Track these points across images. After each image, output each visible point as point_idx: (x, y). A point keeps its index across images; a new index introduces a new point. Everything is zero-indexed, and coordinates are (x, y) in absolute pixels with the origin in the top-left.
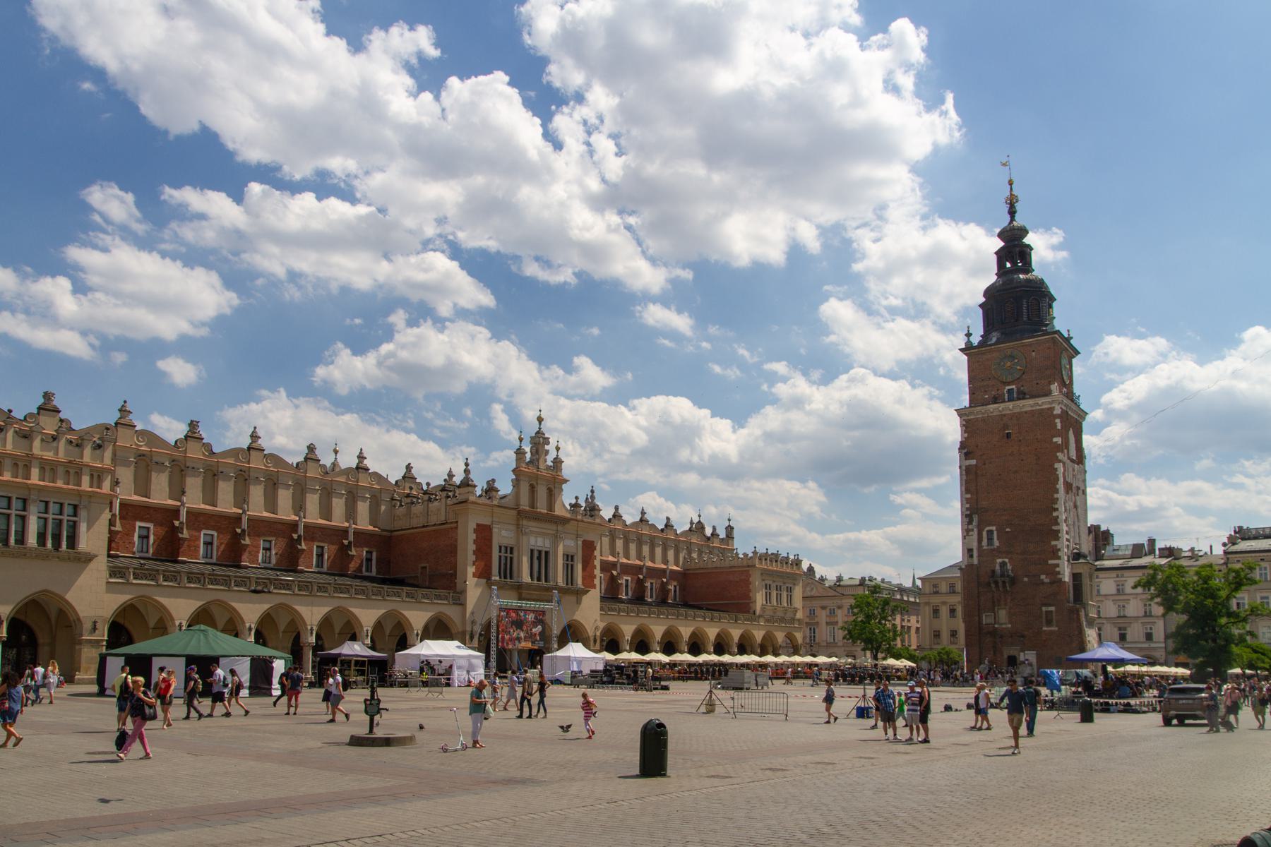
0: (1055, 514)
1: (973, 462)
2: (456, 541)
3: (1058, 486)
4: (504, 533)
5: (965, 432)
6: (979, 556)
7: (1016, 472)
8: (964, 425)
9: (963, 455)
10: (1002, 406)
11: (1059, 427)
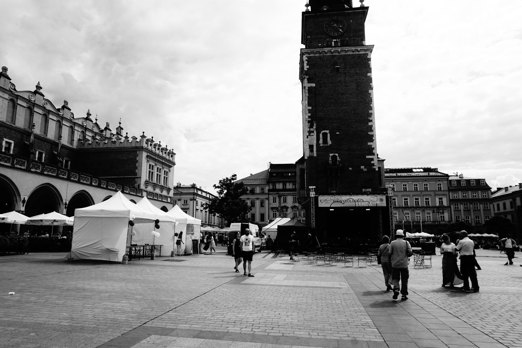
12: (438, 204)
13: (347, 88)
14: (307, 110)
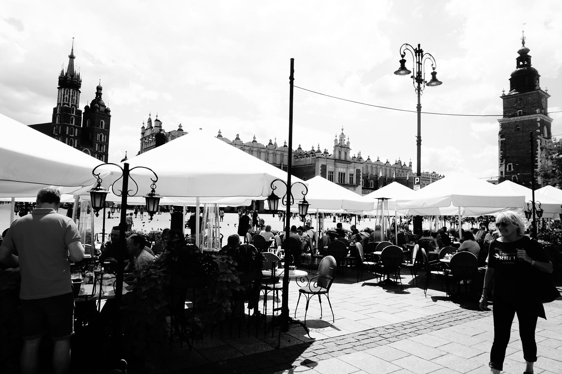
0: (536, 159)
1: (504, 139)
2: (315, 170)
3: (538, 148)
4: (330, 167)
5: (501, 128)
6: (505, 174)
7: (521, 143)
8: (501, 125)
9: (500, 137)
10: (516, 118)
11: (539, 125)
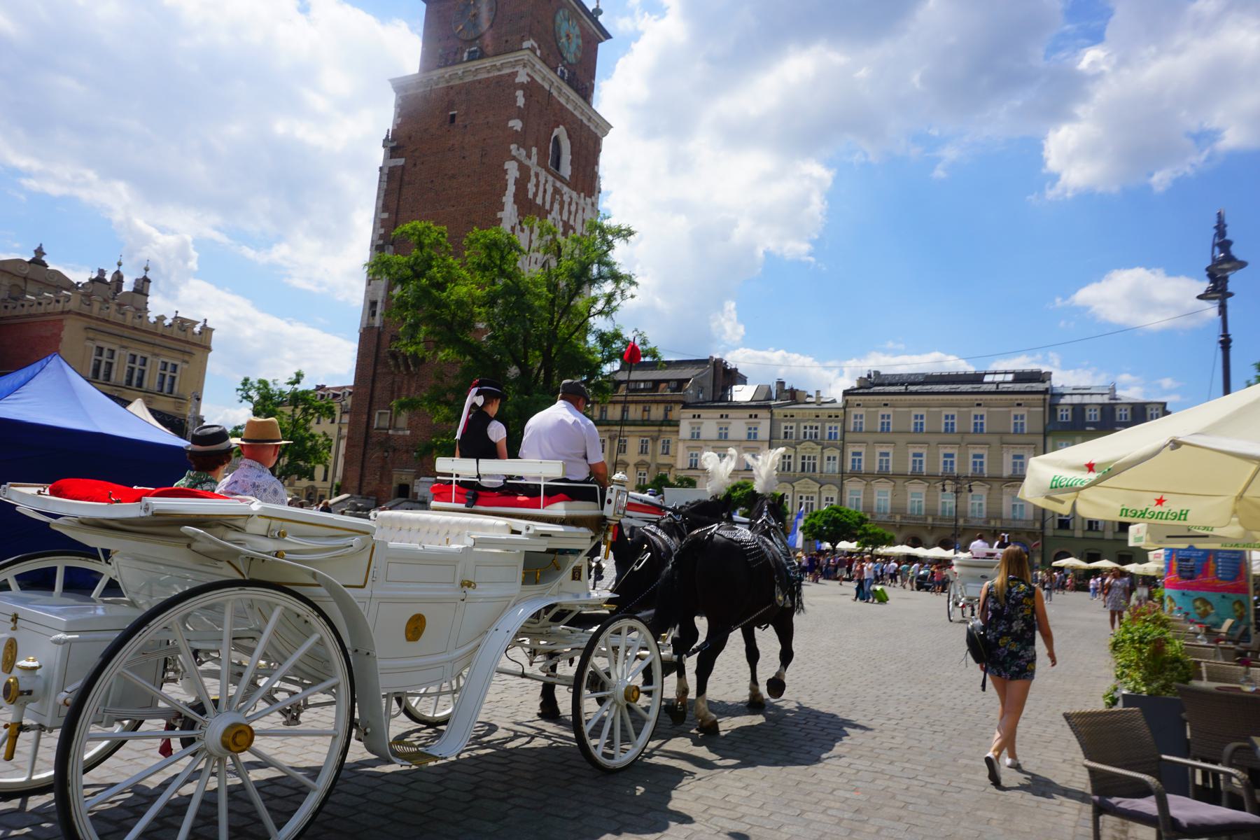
1: (401, 162)
7: (453, 177)
12: (970, 471)
13: (463, 161)
14: (378, 221)
